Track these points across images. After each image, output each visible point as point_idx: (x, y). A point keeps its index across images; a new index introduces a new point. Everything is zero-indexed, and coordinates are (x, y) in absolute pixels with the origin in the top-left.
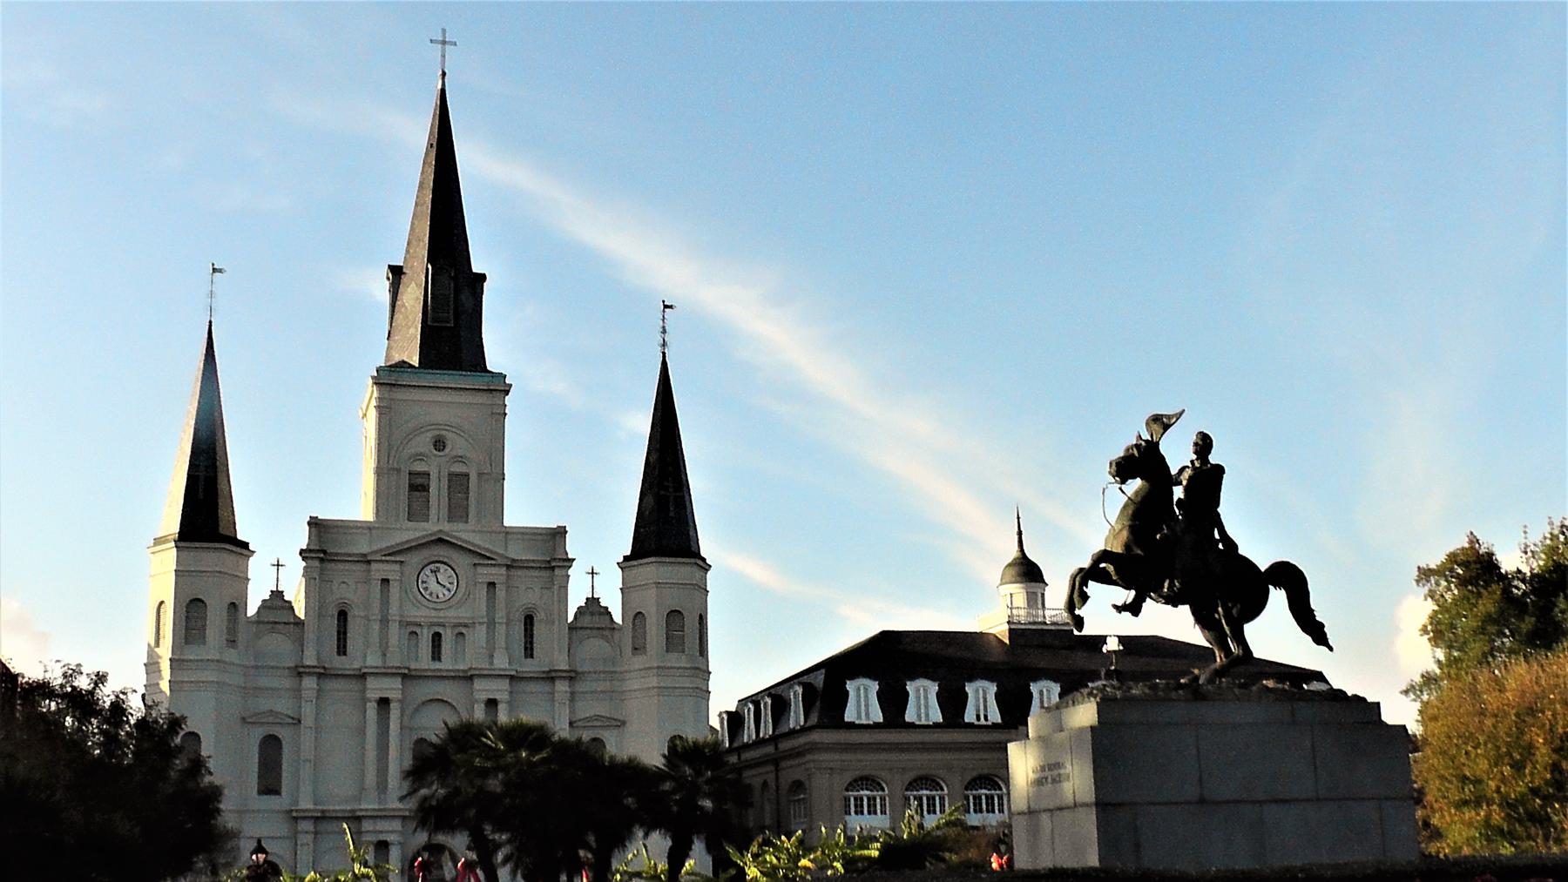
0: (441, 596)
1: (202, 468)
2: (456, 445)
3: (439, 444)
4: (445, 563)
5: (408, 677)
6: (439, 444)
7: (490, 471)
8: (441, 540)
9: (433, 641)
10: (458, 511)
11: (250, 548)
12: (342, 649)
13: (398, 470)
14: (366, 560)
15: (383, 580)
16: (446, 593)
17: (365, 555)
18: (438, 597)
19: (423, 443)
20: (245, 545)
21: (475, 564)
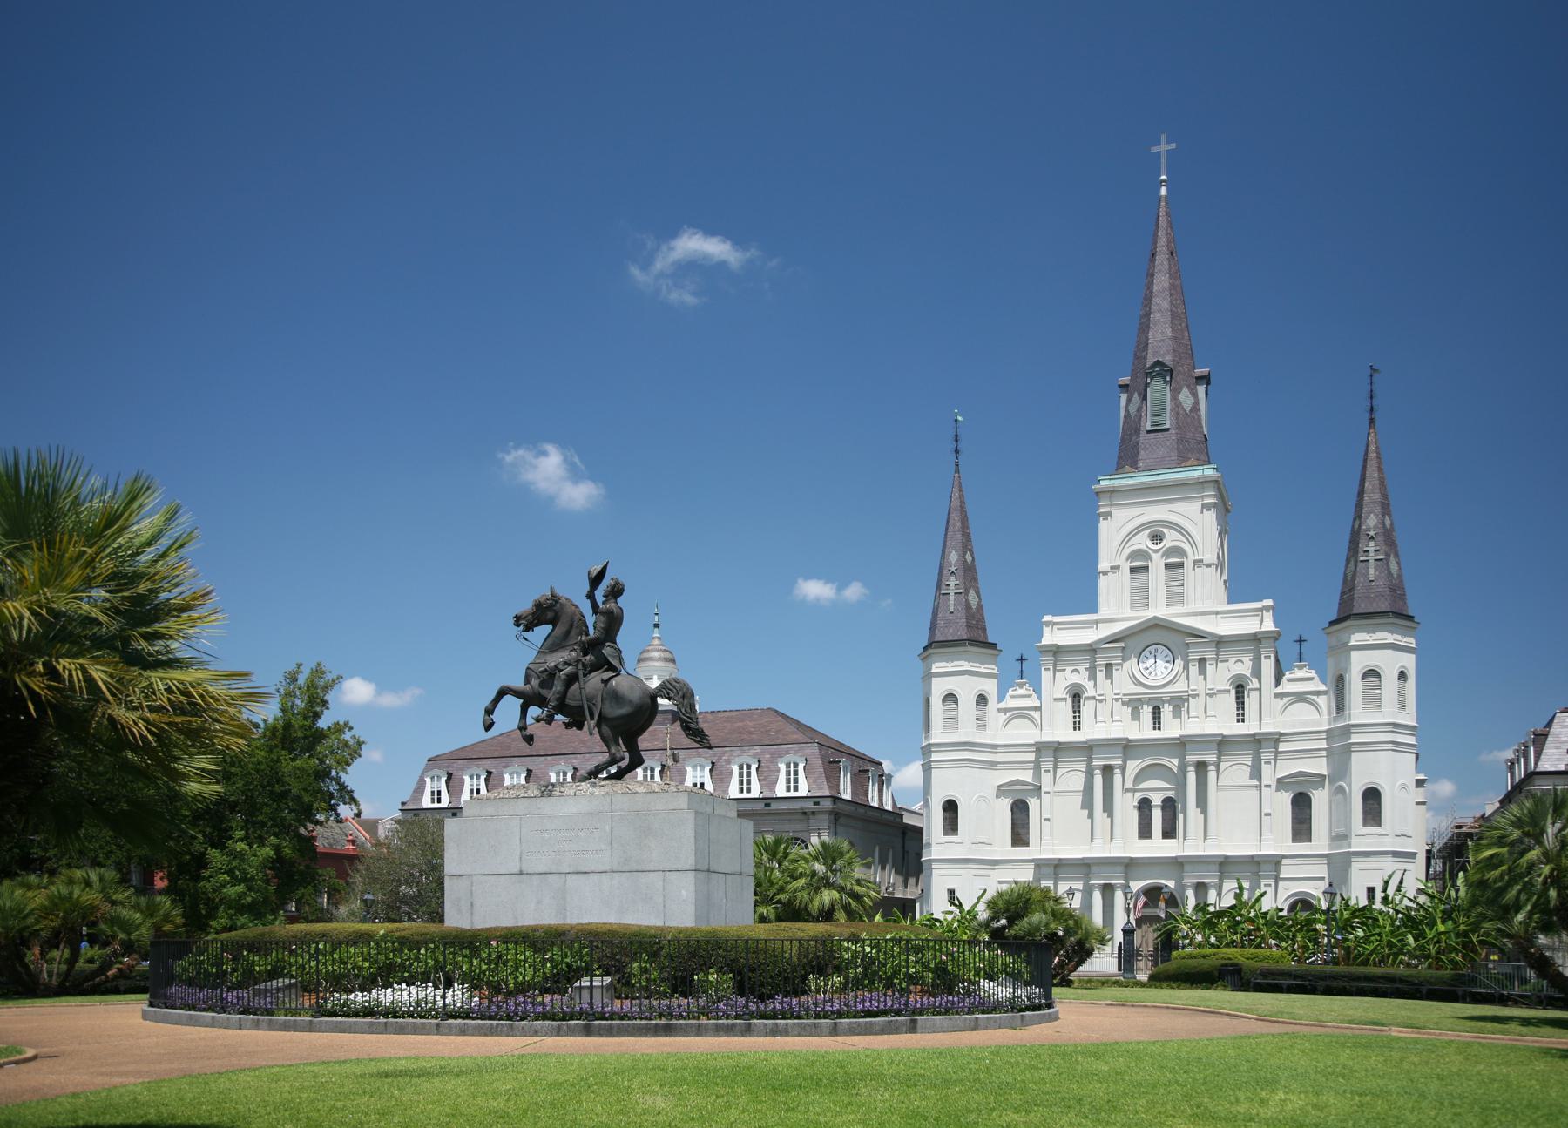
0: (1159, 673)
1: (952, 586)
2: (1171, 539)
3: (1157, 537)
4: (1161, 645)
5: (1128, 748)
6: (1157, 537)
7: (1201, 558)
8: (1156, 625)
9: (1154, 713)
10: (1176, 597)
11: (998, 648)
12: (1077, 726)
13: (1118, 567)
14: (1091, 650)
15: (1107, 664)
16: (1164, 670)
17: (1090, 645)
18: (1156, 674)
19: (1143, 541)
20: (993, 646)
21: (1187, 644)
